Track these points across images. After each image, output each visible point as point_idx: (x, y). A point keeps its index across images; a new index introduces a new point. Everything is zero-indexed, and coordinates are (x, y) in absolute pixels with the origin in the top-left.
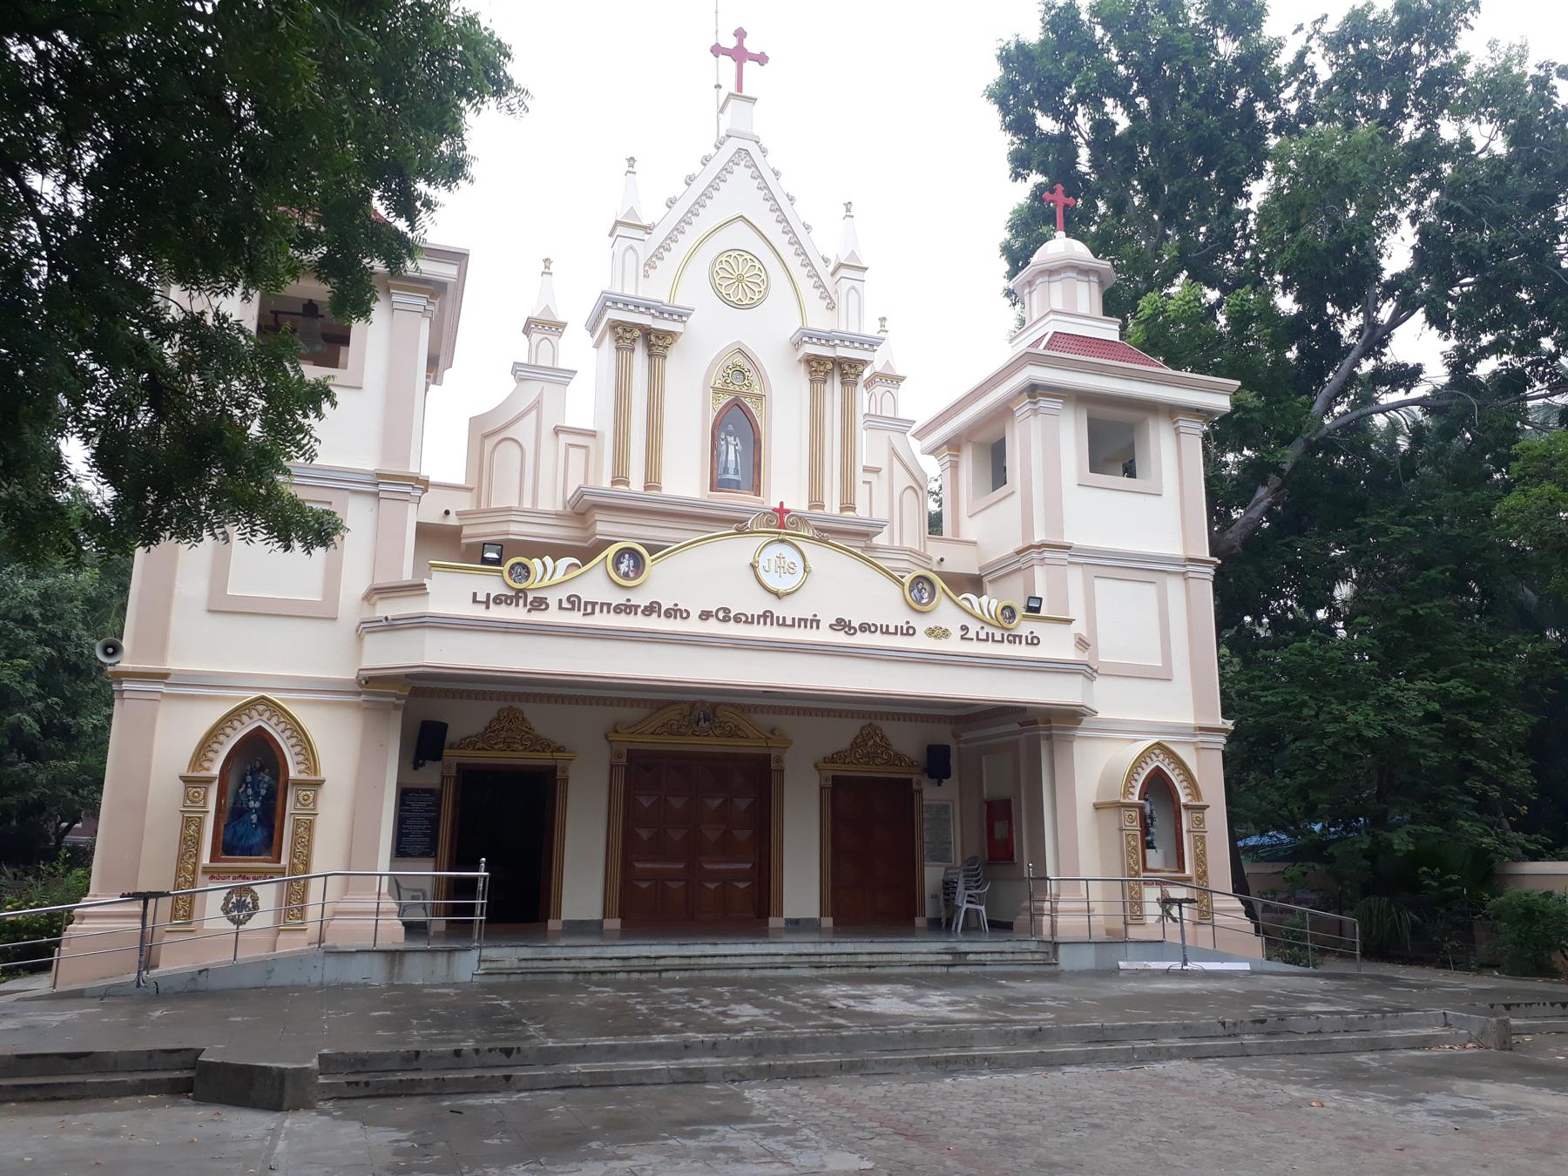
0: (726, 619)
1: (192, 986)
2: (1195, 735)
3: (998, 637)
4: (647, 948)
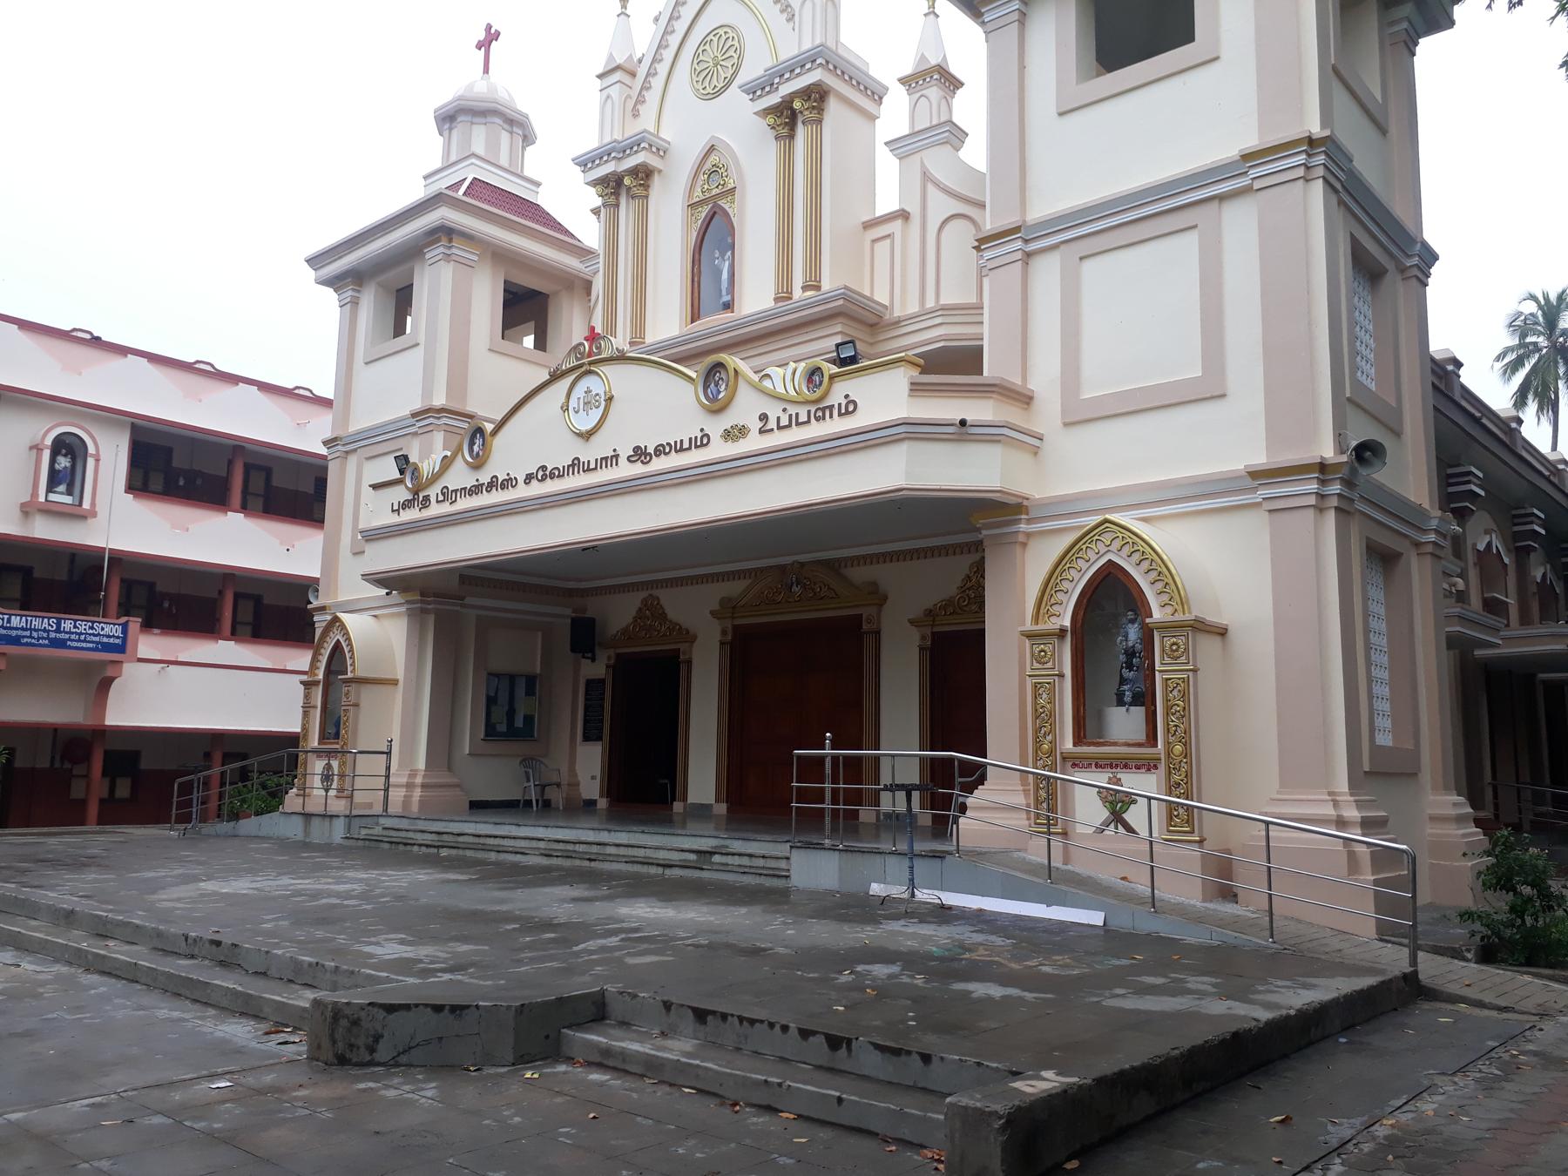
0: (543, 479)
2: (1255, 489)
3: (803, 418)
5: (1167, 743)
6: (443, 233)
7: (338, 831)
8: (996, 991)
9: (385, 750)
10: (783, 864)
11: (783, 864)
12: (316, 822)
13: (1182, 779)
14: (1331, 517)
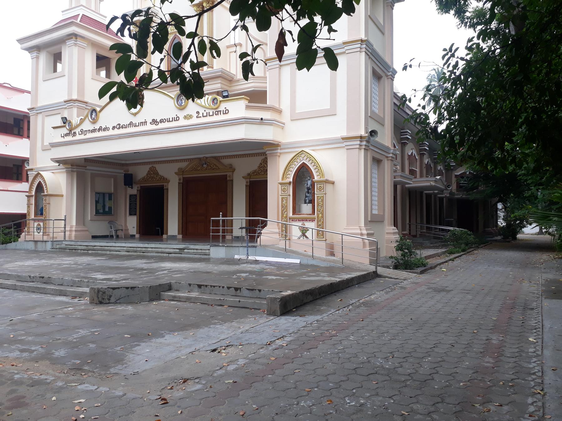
0: (119, 128)
1: (5, 248)
2: (343, 143)
3: (211, 114)
4: (99, 243)
5: (318, 214)
6: (74, 36)
7: (49, 246)
8: (274, 278)
9: (64, 219)
10: (207, 251)
11: (207, 251)
12: (39, 244)
13: (321, 224)
14: (363, 151)
